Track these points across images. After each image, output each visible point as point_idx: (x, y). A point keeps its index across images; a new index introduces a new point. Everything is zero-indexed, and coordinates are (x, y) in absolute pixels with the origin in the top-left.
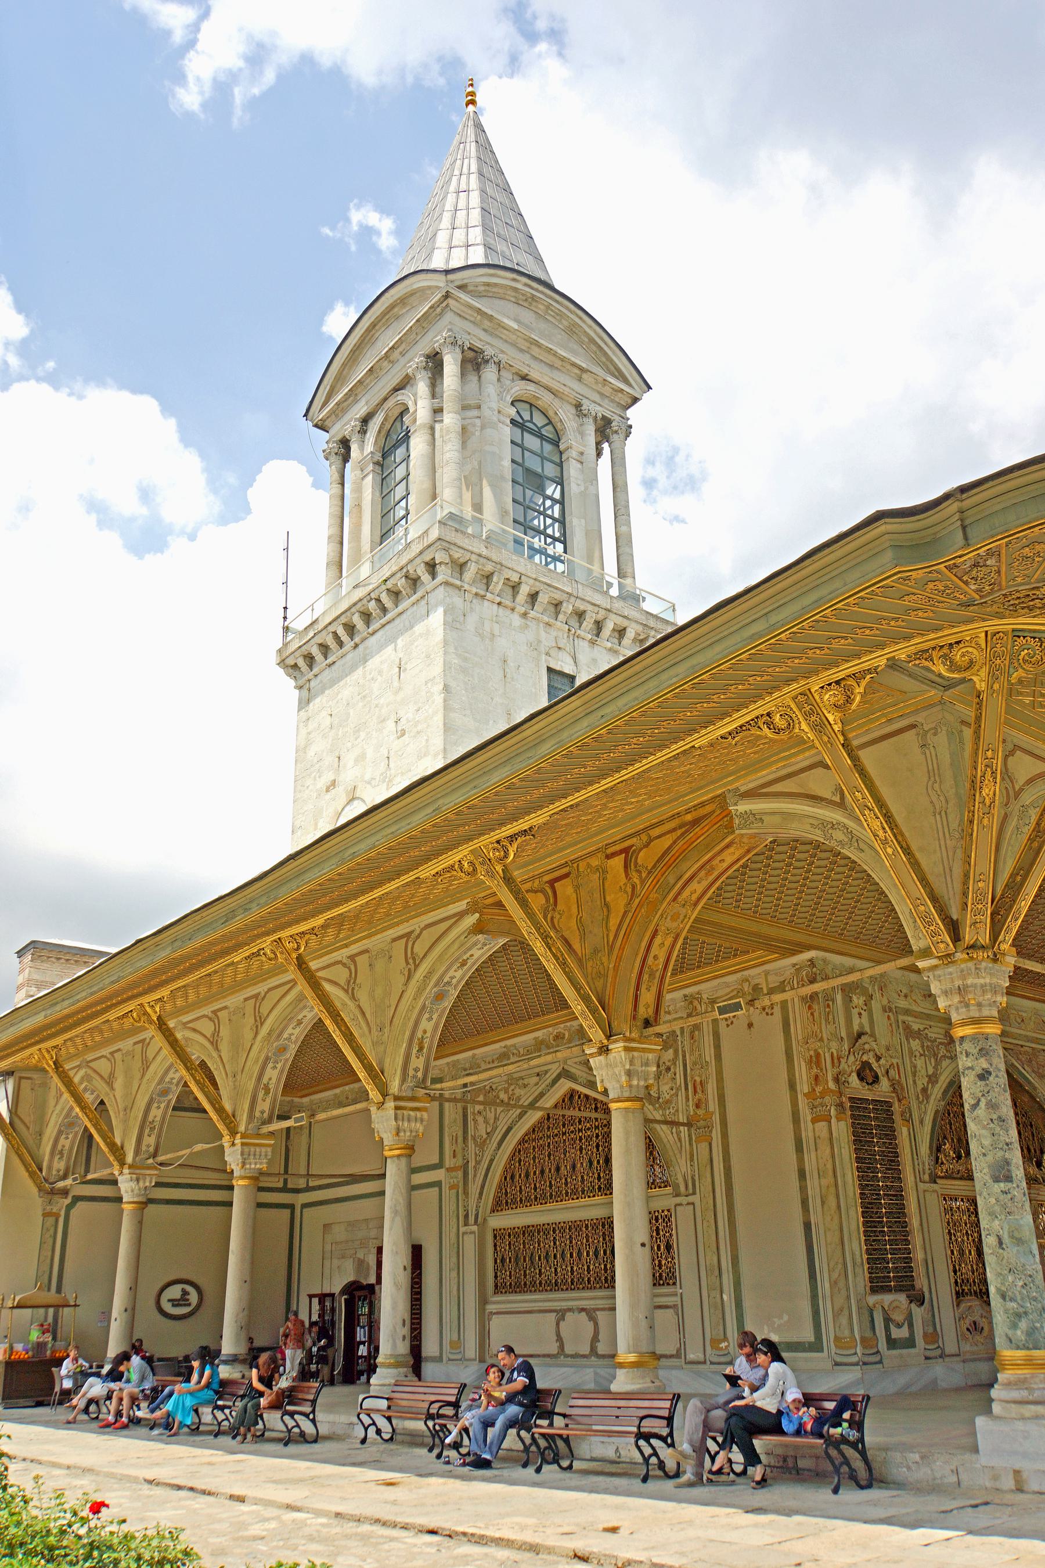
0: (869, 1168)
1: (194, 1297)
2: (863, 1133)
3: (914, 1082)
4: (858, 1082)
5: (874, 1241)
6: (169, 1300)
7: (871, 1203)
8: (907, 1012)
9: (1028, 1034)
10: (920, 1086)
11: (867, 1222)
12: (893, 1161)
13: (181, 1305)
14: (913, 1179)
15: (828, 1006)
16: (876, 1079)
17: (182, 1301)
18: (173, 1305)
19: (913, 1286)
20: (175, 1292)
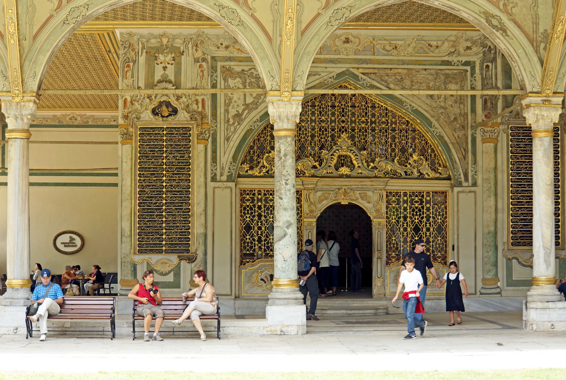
0: (152, 174)
1: (78, 242)
2: (151, 151)
3: (227, 111)
4: (152, 116)
5: (148, 221)
6: (62, 243)
7: (152, 197)
8: (230, 59)
10: (232, 112)
11: (144, 209)
12: (184, 168)
13: (70, 246)
14: (202, 179)
15: (128, 66)
16: (175, 111)
17: (71, 243)
18: (65, 246)
19: (188, 251)
20: (65, 238)
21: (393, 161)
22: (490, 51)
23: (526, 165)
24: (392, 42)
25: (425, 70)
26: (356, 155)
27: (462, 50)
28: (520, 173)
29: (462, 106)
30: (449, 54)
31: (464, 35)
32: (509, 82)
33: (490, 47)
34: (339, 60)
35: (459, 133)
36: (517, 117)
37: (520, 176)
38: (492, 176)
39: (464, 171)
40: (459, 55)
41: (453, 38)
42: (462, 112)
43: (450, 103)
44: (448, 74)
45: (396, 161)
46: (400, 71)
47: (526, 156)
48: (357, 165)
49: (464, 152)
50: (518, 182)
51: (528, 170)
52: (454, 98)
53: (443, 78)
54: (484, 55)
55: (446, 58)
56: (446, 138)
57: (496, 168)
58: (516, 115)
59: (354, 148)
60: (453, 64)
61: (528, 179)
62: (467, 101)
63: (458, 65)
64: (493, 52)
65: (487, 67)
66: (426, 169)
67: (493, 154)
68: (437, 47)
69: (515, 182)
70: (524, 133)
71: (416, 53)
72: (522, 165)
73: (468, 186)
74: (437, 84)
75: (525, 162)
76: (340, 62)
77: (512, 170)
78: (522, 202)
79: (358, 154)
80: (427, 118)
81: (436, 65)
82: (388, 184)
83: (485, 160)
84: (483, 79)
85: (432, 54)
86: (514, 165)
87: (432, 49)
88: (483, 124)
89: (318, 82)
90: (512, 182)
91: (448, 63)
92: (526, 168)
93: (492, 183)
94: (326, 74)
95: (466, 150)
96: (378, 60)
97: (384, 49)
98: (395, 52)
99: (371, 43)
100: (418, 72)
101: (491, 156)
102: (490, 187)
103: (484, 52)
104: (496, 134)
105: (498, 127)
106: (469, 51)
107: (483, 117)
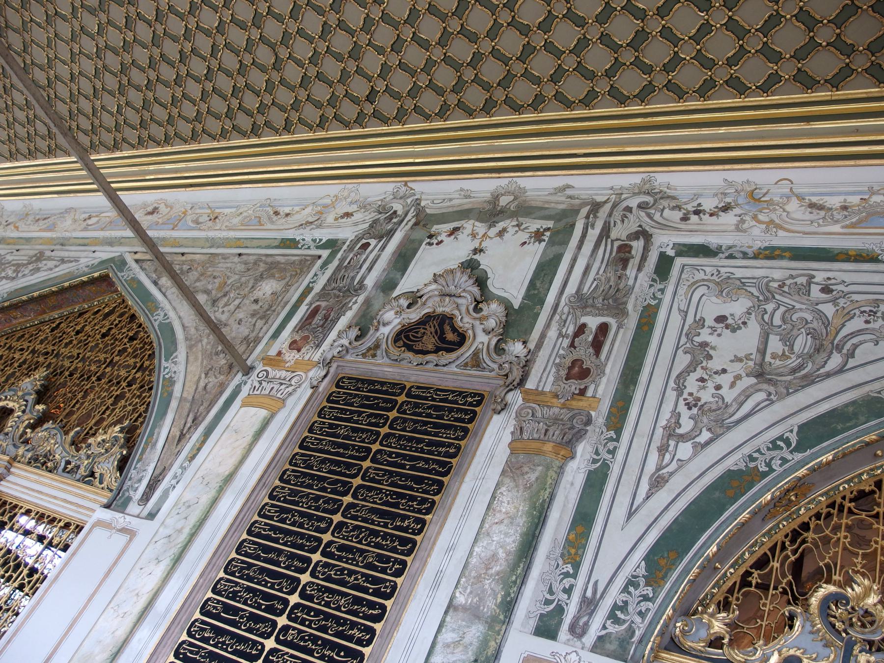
9: (211, 234)
21: (66, 433)
22: (391, 219)
23: (324, 489)
24: (217, 211)
25: (240, 255)
26: (24, 412)
27: (330, 219)
28: (288, 511)
29: (260, 323)
30: (302, 225)
31: (353, 194)
32: (398, 276)
33: (395, 212)
34: (122, 240)
35: (212, 379)
36: (372, 352)
37: (283, 521)
38: (205, 500)
39: (157, 472)
40: (320, 226)
41: (327, 201)
42: (254, 334)
43: (240, 315)
44: (279, 263)
45: (72, 434)
46: (197, 257)
47: (338, 464)
48: (6, 430)
49: (188, 425)
50: (267, 538)
51: (317, 509)
52: (256, 307)
53: (262, 267)
54: (371, 226)
55: (289, 235)
56: (177, 389)
57: (229, 478)
58: (369, 349)
59: (31, 398)
60: (300, 246)
61: (302, 536)
62: (279, 314)
63: (309, 248)
64: (395, 220)
65: (367, 245)
66: (107, 467)
67: (249, 439)
68: (287, 215)
69: (258, 535)
70: (368, 398)
71: (242, 225)
72: (310, 486)
73: (138, 516)
74: (243, 279)
75: (324, 479)
76: (121, 244)
77: (271, 497)
78: (236, 611)
79: (27, 411)
80: (174, 342)
81: (268, 247)
82: (11, 478)
83: (218, 453)
84: (338, 268)
85: (269, 226)
86: (288, 482)
87: (275, 218)
88: (276, 361)
89: (68, 271)
90: (249, 532)
91: (292, 243)
92: (317, 498)
93: (193, 520)
94: (87, 260)
95: (196, 422)
96: (175, 239)
97: (197, 222)
98: (210, 224)
99: (185, 213)
100: (225, 259)
101: (238, 443)
102: (180, 531)
103: (375, 222)
104: (290, 389)
105: (307, 372)
106: (344, 220)
107: (287, 344)
